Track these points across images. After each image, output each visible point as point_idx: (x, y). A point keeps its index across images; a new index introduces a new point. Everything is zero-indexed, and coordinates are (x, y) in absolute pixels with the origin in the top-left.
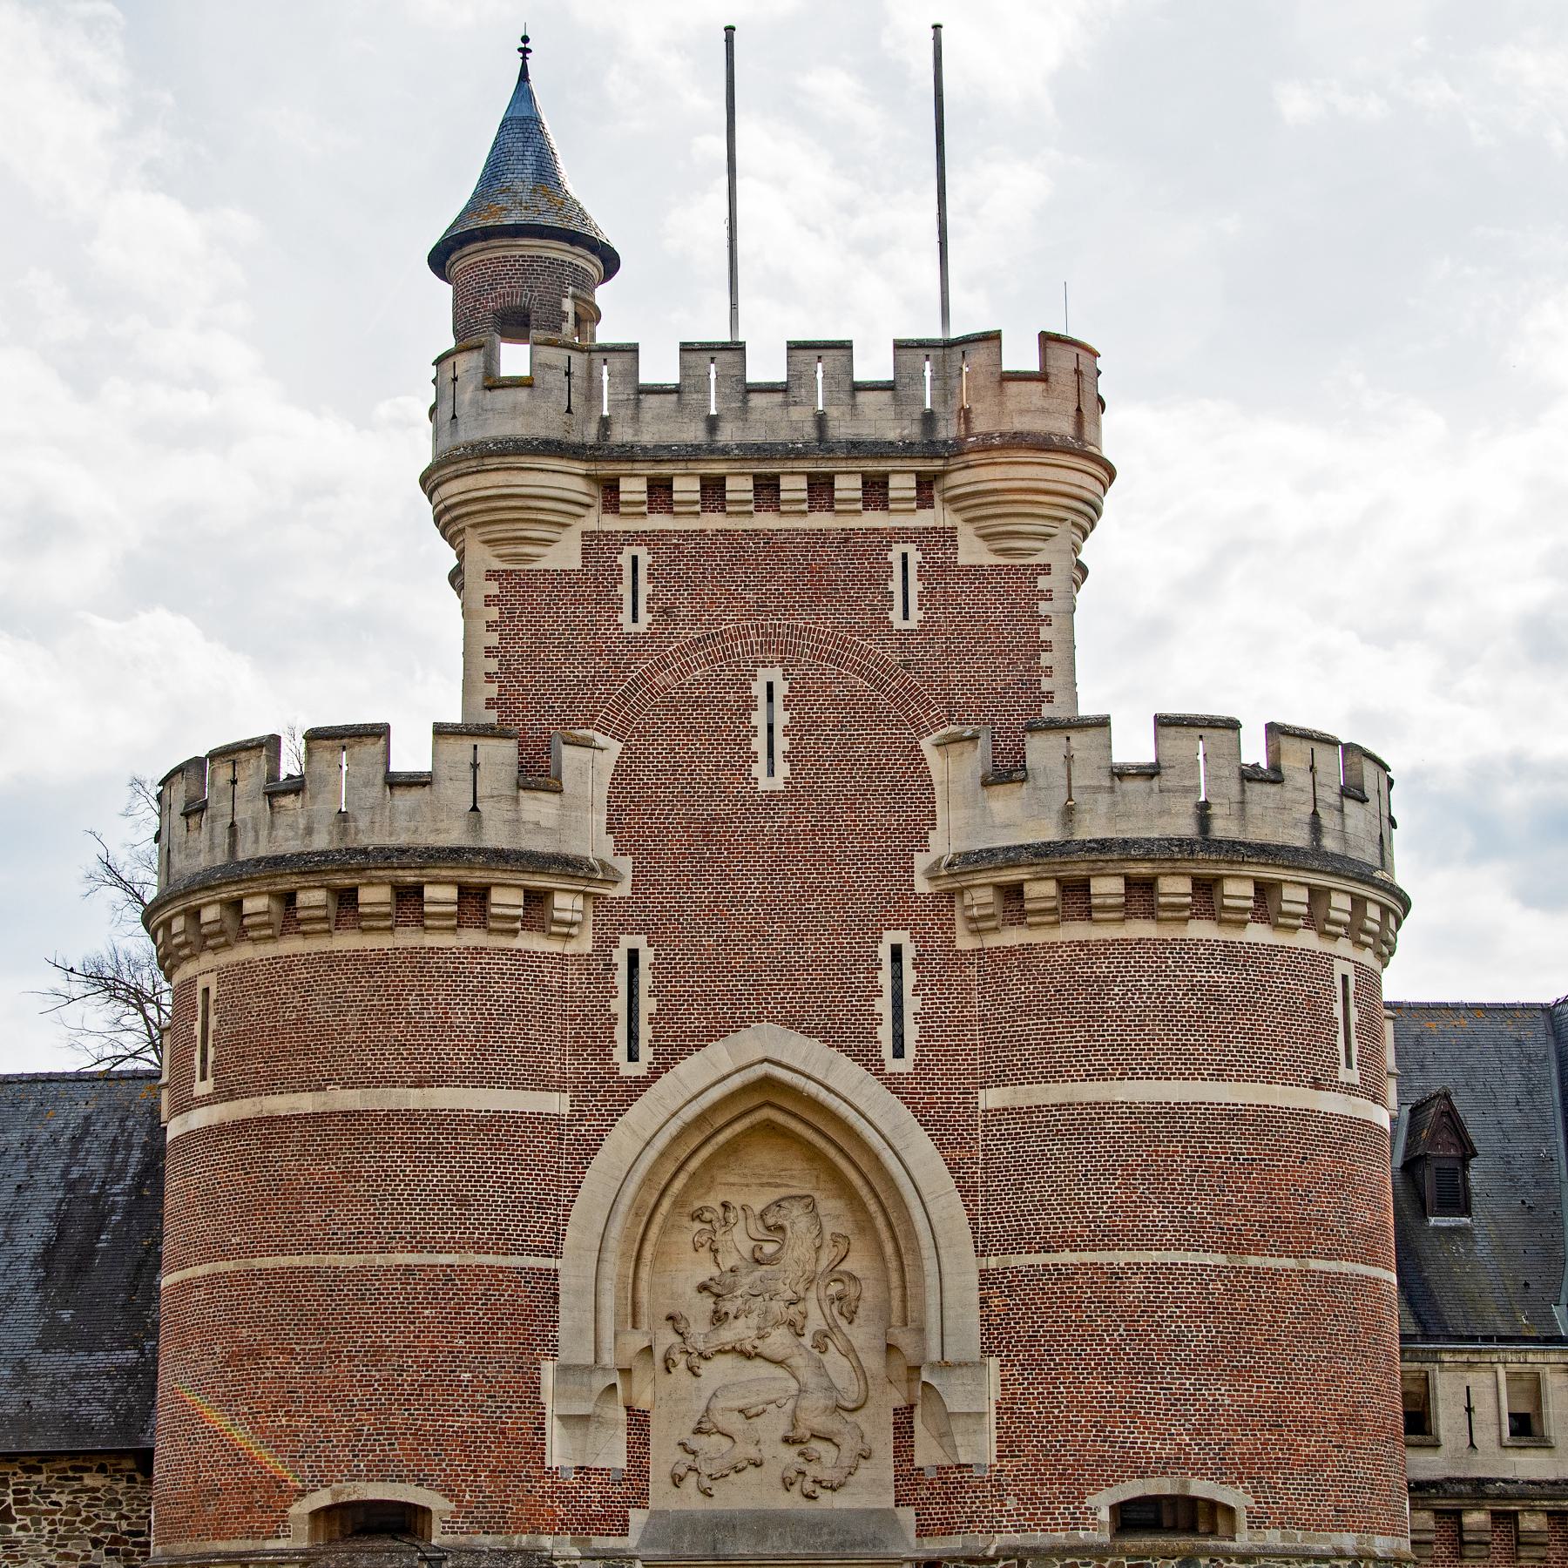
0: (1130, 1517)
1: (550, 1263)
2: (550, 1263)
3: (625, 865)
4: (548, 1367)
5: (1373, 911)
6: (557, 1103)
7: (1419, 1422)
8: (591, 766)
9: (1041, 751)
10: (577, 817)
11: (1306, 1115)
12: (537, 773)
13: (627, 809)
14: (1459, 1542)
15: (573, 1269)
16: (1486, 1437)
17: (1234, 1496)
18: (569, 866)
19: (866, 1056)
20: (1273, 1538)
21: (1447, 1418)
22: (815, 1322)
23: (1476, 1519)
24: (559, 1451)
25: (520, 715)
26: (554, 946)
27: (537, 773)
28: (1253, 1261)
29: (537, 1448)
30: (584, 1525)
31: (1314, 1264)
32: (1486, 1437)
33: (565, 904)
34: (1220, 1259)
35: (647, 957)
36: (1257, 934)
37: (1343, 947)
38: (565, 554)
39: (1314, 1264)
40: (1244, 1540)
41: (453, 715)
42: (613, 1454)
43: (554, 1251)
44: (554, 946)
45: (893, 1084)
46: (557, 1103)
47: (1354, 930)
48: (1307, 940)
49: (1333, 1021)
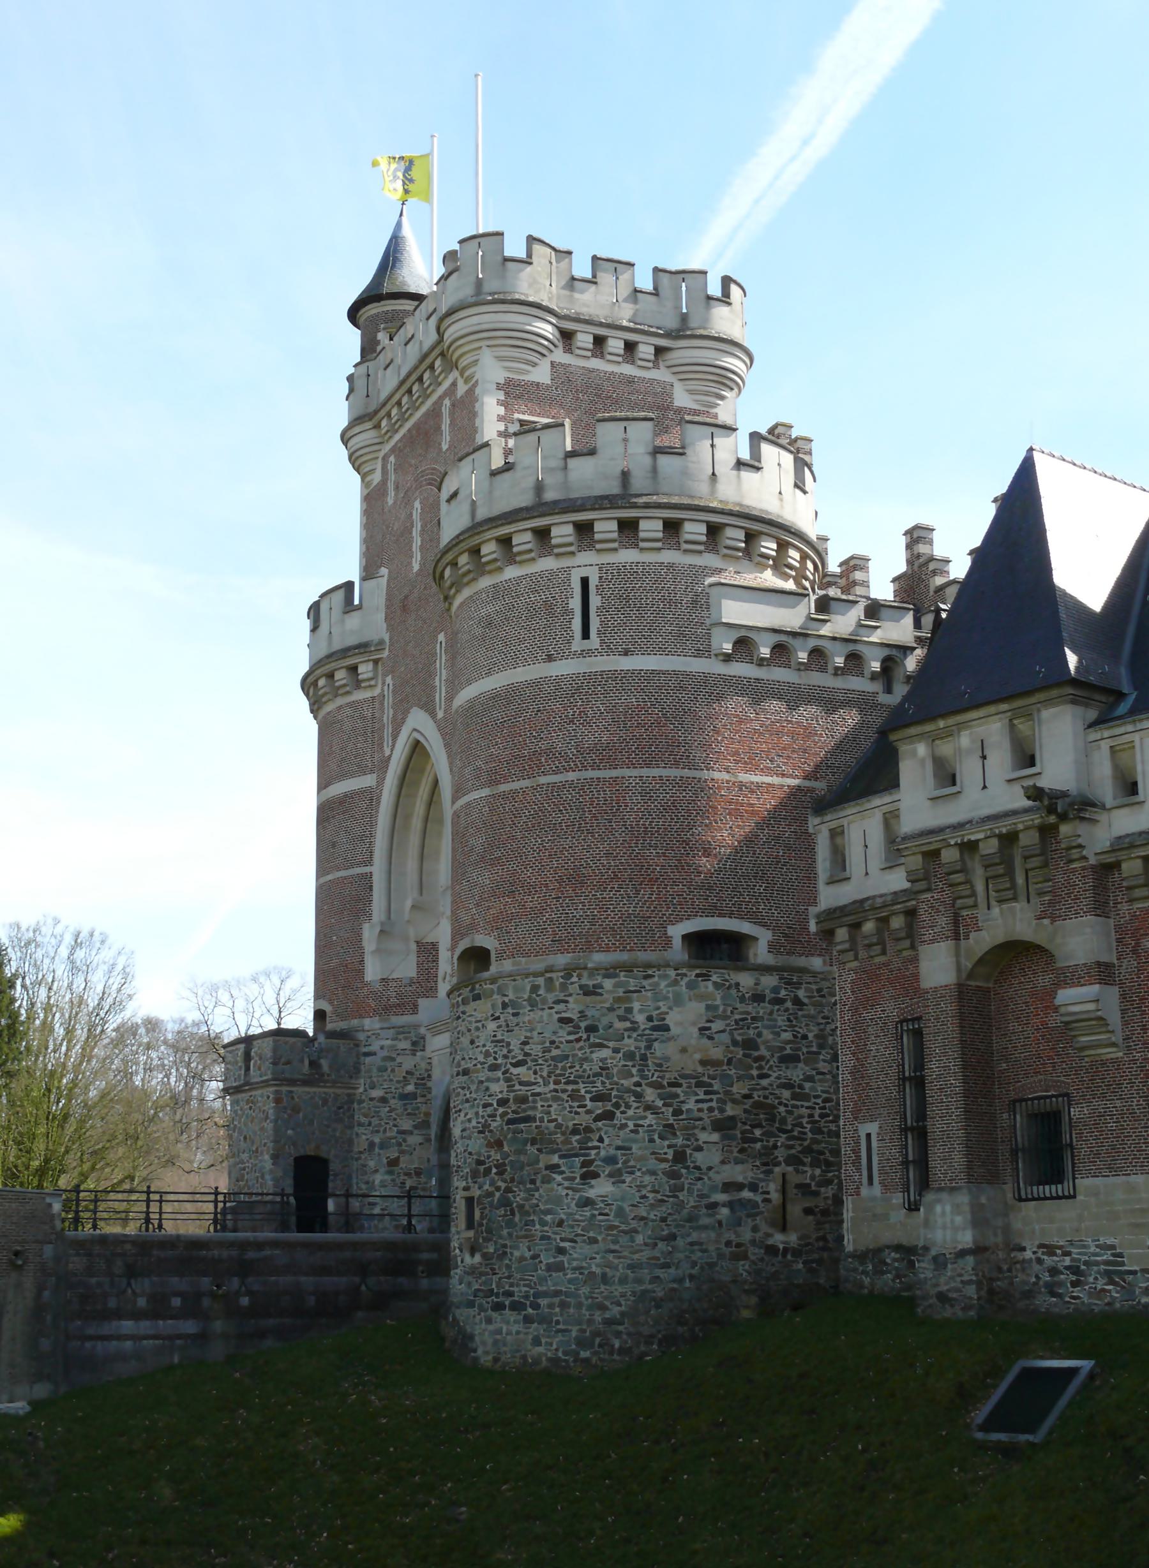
1: (367, 869)
2: (367, 869)
4: (366, 926)
11: (536, 684)
15: (377, 870)
18: (362, 647)
19: (432, 714)
20: (508, 966)
24: (372, 971)
26: (368, 694)
28: (503, 788)
29: (360, 972)
30: (386, 1010)
31: (543, 780)
33: (365, 670)
34: (485, 792)
36: (511, 572)
38: (377, 477)
39: (543, 780)
40: (493, 969)
42: (407, 968)
43: (369, 862)
44: (368, 694)
49: (569, 612)
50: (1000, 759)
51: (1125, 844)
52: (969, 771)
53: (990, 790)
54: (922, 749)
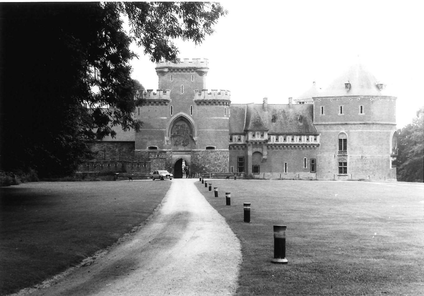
0: (208, 148)
3: (171, 100)
5: (228, 103)
6: (165, 118)
7: (231, 139)
8: (168, 93)
9: (203, 92)
10: (167, 97)
12: (165, 92)
13: (172, 95)
14: (234, 149)
16: (236, 140)
17: (215, 147)
19: (189, 114)
20: (217, 150)
21: (234, 140)
22: (185, 134)
23: (235, 147)
25: (163, 88)
27: (165, 92)
32: (236, 140)
35: (173, 107)
37: (225, 106)
41: (158, 89)
45: (191, 117)
46: (165, 118)
47: (226, 105)
48: (222, 106)
50: (260, 136)
51: (269, 145)
52: (256, 136)
53: (258, 138)
54: (251, 132)
